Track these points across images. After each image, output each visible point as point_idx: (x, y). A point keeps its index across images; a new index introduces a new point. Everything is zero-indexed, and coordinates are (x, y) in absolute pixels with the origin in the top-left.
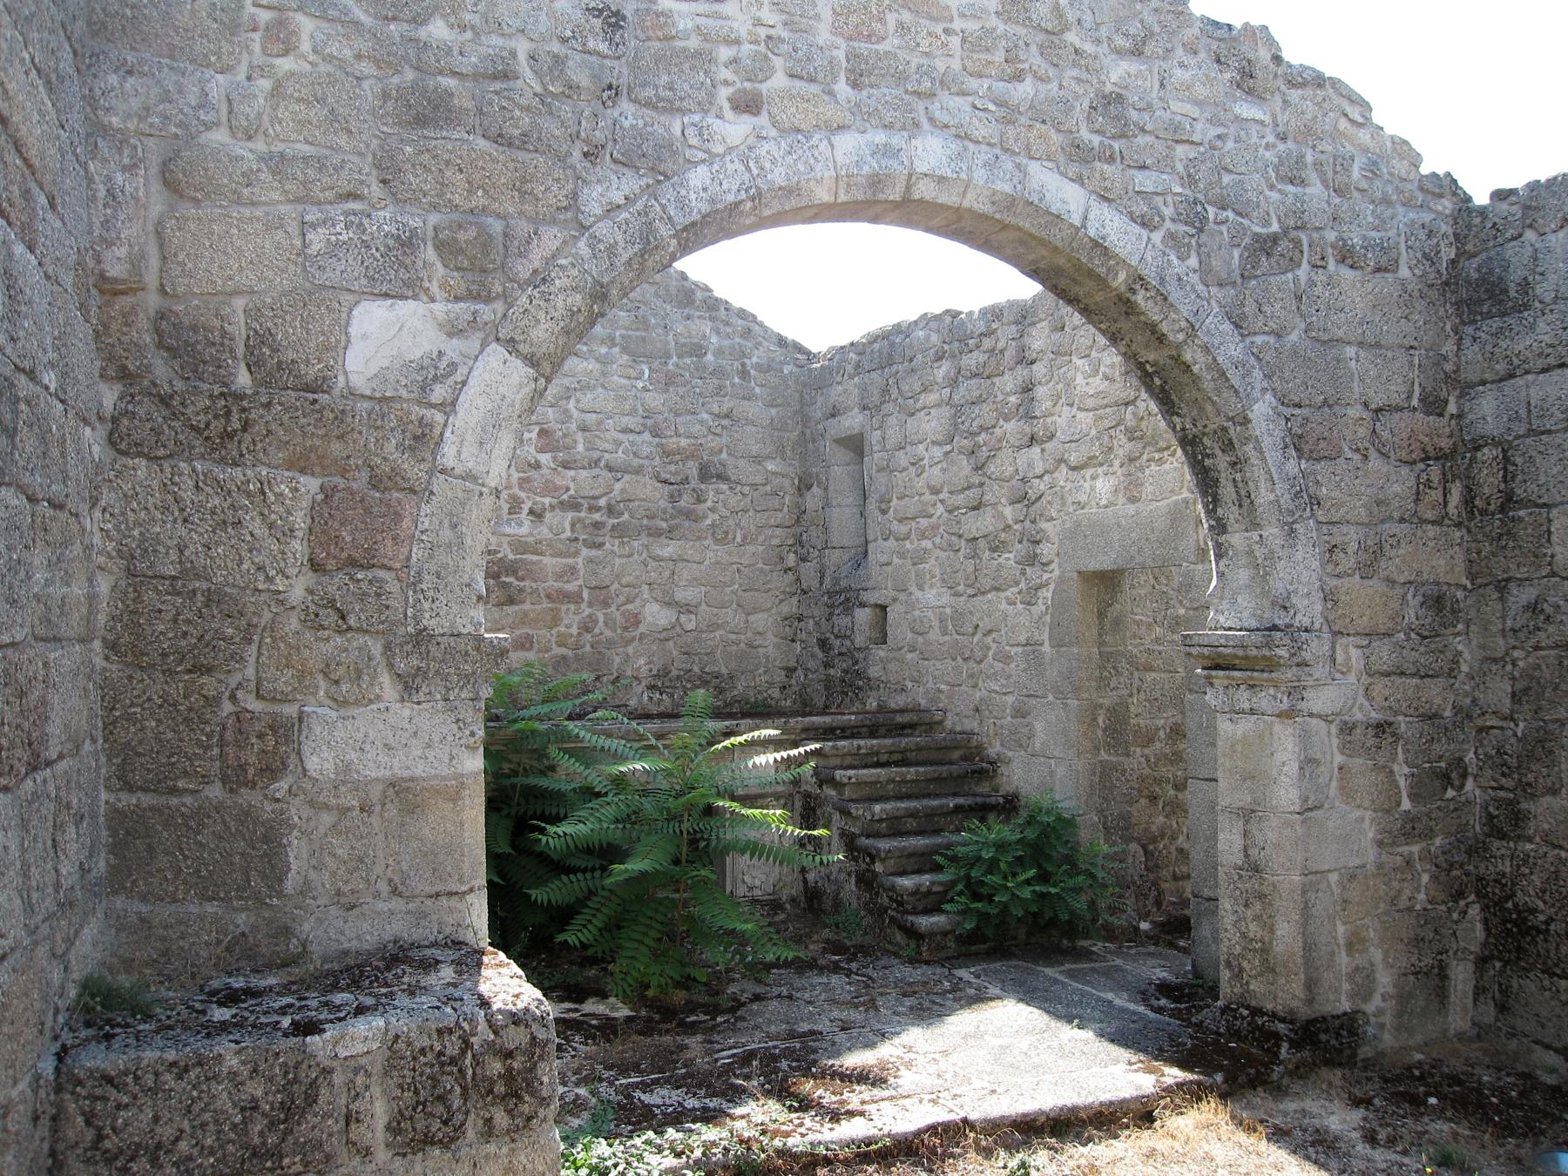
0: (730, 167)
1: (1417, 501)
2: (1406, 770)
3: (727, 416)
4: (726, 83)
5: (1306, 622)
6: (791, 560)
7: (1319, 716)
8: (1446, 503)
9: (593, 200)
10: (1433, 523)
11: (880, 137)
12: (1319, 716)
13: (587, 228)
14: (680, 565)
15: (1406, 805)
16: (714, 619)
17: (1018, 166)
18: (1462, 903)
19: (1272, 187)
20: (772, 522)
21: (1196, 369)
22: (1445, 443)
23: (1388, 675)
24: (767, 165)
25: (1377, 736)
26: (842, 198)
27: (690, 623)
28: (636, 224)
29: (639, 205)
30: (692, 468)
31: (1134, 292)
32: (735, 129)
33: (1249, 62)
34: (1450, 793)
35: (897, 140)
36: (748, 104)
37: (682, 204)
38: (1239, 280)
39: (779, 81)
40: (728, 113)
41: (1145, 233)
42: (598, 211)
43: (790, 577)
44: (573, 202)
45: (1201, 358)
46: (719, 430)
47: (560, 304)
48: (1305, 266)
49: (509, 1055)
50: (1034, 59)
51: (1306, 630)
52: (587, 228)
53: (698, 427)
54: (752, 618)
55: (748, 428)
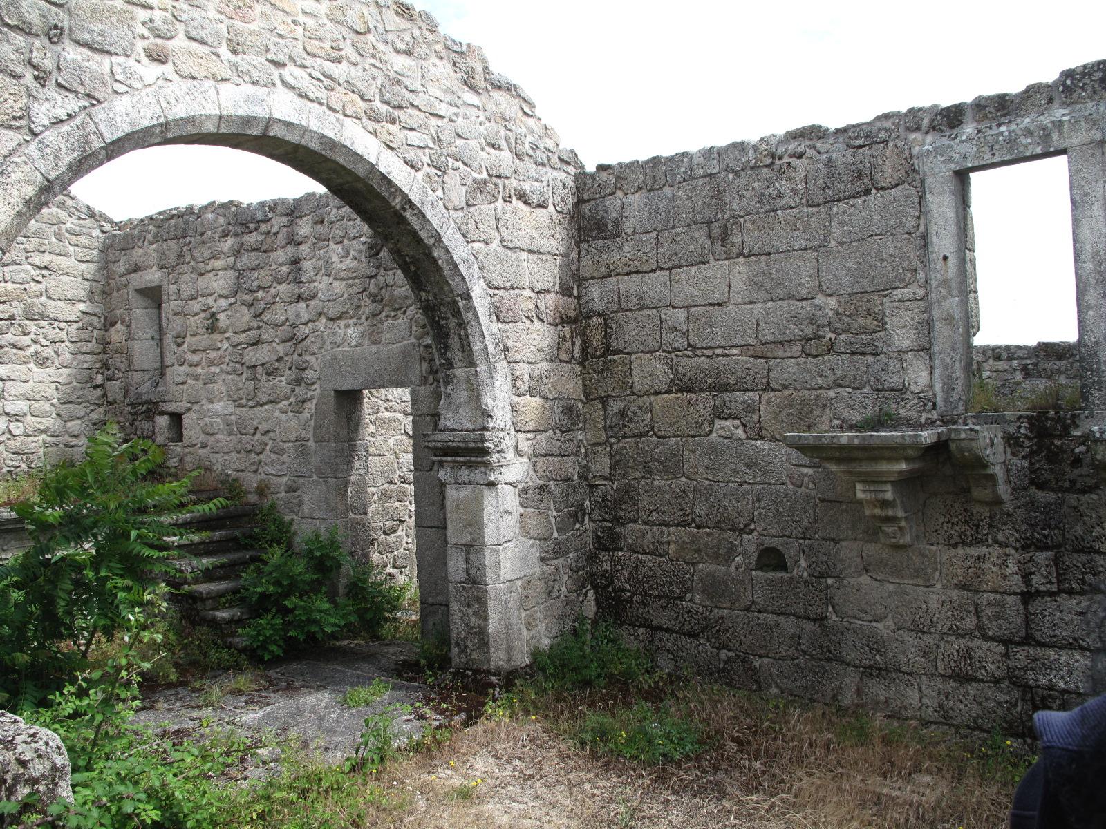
0: (146, 100)
1: (558, 348)
2: (555, 514)
3: (46, 268)
4: (143, 37)
5: (502, 425)
6: (99, 379)
7: (511, 484)
8: (573, 350)
9: (42, 113)
10: (567, 362)
11: (250, 89)
12: (511, 484)
13: (36, 135)
14: (9, 383)
15: (555, 535)
16: (39, 427)
17: (338, 120)
18: (584, 591)
19: (483, 149)
20: (83, 350)
21: (440, 262)
22: (572, 314)
23: (545, 455)
24: (173, 101)
25: (540, 494)
26: (223, 130)
27: (17, 428)
28: (76, 136)
29: (77, 121)
30: (17, 309)
31: (405, 210)
32: (152, 71)
33: (472, 68)
34: (578, 526)
35: (261, 92)
36: (158, 58)
37: (111, 124)
38: (465, 207)
39: (180, 42)
40: (145, 60)
41: (413, 171)
42: (47, 123)
43: (99, 392)
44: (27, 114)
45: (442, 254)
46: (39, 279)
47: (15, 193)
48: (500, 200)
49: (36, 781)
50: (348, 51)
51: (503, 430)
52: (36, 135)
53: (22, 275)
54: (69, 424)
55: (65, 278)
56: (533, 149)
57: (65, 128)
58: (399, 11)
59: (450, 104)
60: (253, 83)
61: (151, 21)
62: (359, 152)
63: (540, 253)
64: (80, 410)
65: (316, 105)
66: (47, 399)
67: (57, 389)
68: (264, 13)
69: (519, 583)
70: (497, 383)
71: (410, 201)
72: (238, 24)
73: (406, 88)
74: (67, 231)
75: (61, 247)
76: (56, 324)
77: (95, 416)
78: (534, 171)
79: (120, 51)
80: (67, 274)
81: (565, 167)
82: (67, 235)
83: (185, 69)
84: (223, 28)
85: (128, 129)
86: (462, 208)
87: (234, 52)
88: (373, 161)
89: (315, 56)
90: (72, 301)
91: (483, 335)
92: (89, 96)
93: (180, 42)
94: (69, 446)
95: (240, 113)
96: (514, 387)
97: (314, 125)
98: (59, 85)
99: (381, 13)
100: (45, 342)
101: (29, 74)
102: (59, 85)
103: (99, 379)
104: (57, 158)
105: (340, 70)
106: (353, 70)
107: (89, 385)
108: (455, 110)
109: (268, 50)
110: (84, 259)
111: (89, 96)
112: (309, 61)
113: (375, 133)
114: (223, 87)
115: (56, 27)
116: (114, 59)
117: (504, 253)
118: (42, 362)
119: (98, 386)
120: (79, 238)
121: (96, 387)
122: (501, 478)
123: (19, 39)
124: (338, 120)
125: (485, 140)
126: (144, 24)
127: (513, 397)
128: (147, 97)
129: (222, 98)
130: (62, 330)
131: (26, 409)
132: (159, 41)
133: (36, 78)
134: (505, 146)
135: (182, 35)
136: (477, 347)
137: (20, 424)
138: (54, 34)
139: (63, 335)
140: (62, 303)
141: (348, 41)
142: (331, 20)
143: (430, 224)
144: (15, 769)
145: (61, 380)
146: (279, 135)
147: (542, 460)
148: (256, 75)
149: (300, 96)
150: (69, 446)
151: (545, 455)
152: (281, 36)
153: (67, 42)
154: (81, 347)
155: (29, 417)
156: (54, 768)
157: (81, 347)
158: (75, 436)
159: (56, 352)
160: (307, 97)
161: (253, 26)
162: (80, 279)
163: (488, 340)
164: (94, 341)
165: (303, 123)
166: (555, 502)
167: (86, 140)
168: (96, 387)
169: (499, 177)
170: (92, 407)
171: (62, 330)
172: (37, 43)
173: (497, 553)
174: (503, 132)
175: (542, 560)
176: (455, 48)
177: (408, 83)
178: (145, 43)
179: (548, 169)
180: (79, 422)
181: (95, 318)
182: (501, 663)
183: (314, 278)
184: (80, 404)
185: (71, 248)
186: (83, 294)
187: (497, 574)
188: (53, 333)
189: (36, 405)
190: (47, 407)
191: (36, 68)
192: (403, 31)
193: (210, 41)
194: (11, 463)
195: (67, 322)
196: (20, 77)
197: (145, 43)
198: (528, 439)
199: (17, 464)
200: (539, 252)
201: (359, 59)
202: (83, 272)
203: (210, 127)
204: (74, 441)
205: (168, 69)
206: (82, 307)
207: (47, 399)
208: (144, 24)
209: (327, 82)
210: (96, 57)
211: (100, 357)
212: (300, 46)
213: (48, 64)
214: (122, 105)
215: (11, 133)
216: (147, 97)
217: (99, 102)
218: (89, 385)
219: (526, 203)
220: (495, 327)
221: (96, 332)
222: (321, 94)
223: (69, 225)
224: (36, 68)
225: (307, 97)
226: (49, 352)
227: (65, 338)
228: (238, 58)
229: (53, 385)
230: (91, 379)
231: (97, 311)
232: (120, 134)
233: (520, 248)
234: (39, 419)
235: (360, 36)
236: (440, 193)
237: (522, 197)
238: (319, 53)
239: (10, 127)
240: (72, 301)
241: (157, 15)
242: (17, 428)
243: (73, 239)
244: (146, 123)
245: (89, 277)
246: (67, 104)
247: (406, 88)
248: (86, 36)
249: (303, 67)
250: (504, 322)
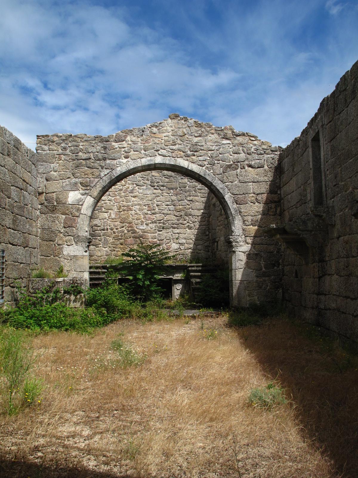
0: (124, 167)
1: (268, 211)
2: (264, 263)
3: (191, 201)
4: (123, 154)
5: (238, 234)
6: (207, 233)
7: (242, 252)
8: (276, 211)
9: (102, 174)
10: (273, 215)
11: (149, 158)
12: (242, 252)
13: (101, 178)
14: (180, 235)
15: (264, 269)
16: (189, 247)
17: (175, 159)
18: (278, 290)
19: (231, 155)
20: (202, 224)
21: (214, 190)
22: (276, 199)
23: (259, 244)
24: (130, 165)
25: (256, 256)
26: (144, 168)
27: (182, 247)
28: (109, 177)
29: (109, 174)
30: (183, 213)
31: (200, 178)
32: (125, 161)
33: (226, 133)
34: (275, 268)
35: (152, 158)
36: (126, 157)
37: (116, 173)
38: (222, 173)
39: (132, 152)
40: (123, 158)
41: (201, 167)
42: (103, 176)
43: (207, 237)
44: (100, 175)
45: (214, 187)
46: (189, 204)
47: (98, 189)
48: (239, 169)
49: (78, 284)
50: (179, 142)
51: (238, 236)
52: (101, 178)
53: (184, 203)
54: (198, 247)
55: (197, 203)
56: (256, 150)
57: (107, 176)
58: (197, 126)
59: (216, 146)
60: (150, 157)
61: (125, 150)
62: (182, 166)
63: (259, 182)
64: (201, 242)
65: (168, 157)
66: (191, 239)
67: (194, 236)
68: (153, 140)
69: (245, 282)
70: (236, 222)
71: (200, 175)
72: (146, 144)
73: (199, 145)
74: (198, 189)
75: (196, 194)
76: (194, 217)
77: (206, 244)
78: (256, 156)
79: (118, 158)
80: (198, 202)
81: (274, 153)
82: (198, 190)
83: (132, 158)
84: (142, 147)
85: (120, 173)
86: (221, 174)
87: (145, 151)
88: (186, 167)
89: (167, 146)
90: (199, 210)
91: (230, 209)
92: (111, 169)
93: (132, 152)
94: (198, 253)
95: (147, 164)
96: (244, 223)
97: (167, 162)
98: (106, 168)
99: (190, 129)
100: (191, 222)
101: (100, 168)
102: (106, 168)
103: (207, 233)
104: (106, 182)
105: (177, 147)
106: (180, 146)
107: (204, 235)
108: (219, 147)
109: (154, 148)
110: (203, 197)
111: (111, 169)
112: (166, 147)
113: (187, 160)
114: (142, 160)
115: (105, 158)
116: (117, 160)
117: (240, 184)
118: (190, 228)
119: (207, 235)
120: (201, 191)
121: (207, 235)
122: (237, 250)
123: (98, 162)
124: (175, 159)
125: (232, 152)
126: (123, 151)
127: (244, 226)
128: (124, 166)
129: (142, 162)
130: (196, 218)
131: (185, 242)
132: (127, 154)
133: (101, 168)
134: (242, 152)
135: (132, 151)
136: (229, 212)
137: (183, 246)
138: (105, 159)
139: (196, 220)
140: (196, 210)
141: (178, 139)
142: (172, 136)
143: (208, 180)
144: (75, 281)
145: (195, 233)
146: (159, 166)
147: (257, 246)
148: (151, 155)
149: (163, 156)
150: (198, 253)
151: (259, 244)
152: (158, 144)
153: (107, 159)
154: (202, 223)
155: (186, 244)
156: (81, 283)
157: (202, 223)
158: (200, 250)
159: (194, 225)
160: (165, 156)
161: (150, 144)
162: (202, 203)
163: (232, 210)
164: (206, 221)
165: (164, 162)
166: (263, 259)
167: (111, 177)
168: (207, 235)
169: (238, 162)
170: (205, 242)
171: (196, 218)
172: (101, 161)
173: (235, 271)
174: (241, 148)
175: (257, 276)
176: (219, 129)
177: (200, 144)
178: (124, 155)
179: (265, 155)
180: (201, 246)
181: (206, 214)
182: (236, 304)
183: (28, 205)
184: (201, 240)
185: (199, 194)
186: (202, 207)
187: (236, 278)
188: (194, 219)
189: (188, 241)
190: (191, 241)
191: (101, 166)
192: (198, 131)
193: (139, 150)
194: (180, 257)
195: (197, 216)
196: (98, 169)
197: (124, 155)
198: (251, 239)
199: (182, 257)
200: (258, 182)
201: (182, 143)
202: (202, 201)
203: (140, 169)
204: (199, 252)
205: (129, 159)
206: (202, 211)
207: (191, 239)
208: (123, 151)
209: (172, 151)
210: (113, 161)
211: (208, 226)
212: (163, 145)
213: (103, 165)
214: (119, 169)
215: (97, 179)
216: (124, 166)
217: (114, 169)
218: (204, 235)
219: (252, 167)
220: (235, 206)
221: (206, 218)
222: (170, 154)
223: (198, 187)
224: (101, 166)
225: (165, 156)
226: (192, 225)
227: (197, 221)
228: (146, 152)
229: (193, 235)
230: (205, 233)
231: (207, 212)
232: (118, 175)
233: (248, 182)
234: (189, 245)
235: (183, 137)
236: (212, 171)
237: (250, 166)
238: (169, 145)
239: (97, 178)
240: (199, 210)
241: (126, 149)
242: (182, 247)
243: (200, 191)
244: (124, 171)
245: (204, 202)
246: (107, 171)
247: (199, 145)
248: (111, 158)
249: (164, 149)
250: (240, 204)
